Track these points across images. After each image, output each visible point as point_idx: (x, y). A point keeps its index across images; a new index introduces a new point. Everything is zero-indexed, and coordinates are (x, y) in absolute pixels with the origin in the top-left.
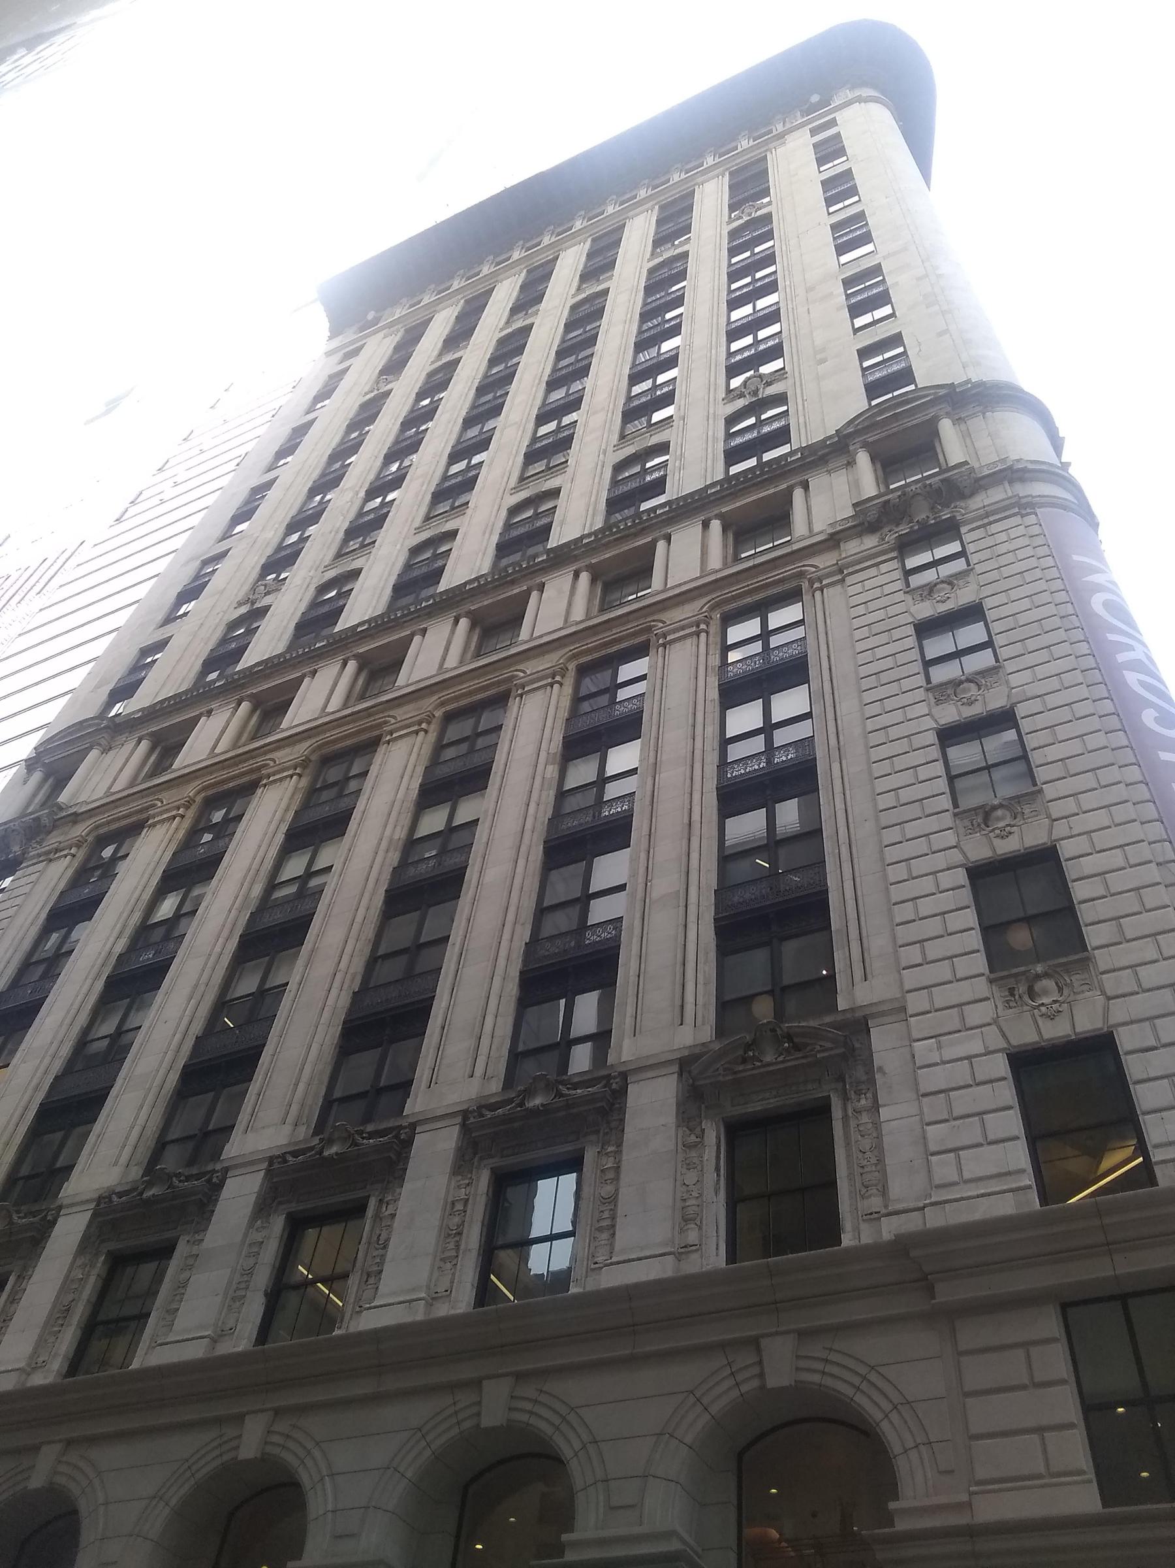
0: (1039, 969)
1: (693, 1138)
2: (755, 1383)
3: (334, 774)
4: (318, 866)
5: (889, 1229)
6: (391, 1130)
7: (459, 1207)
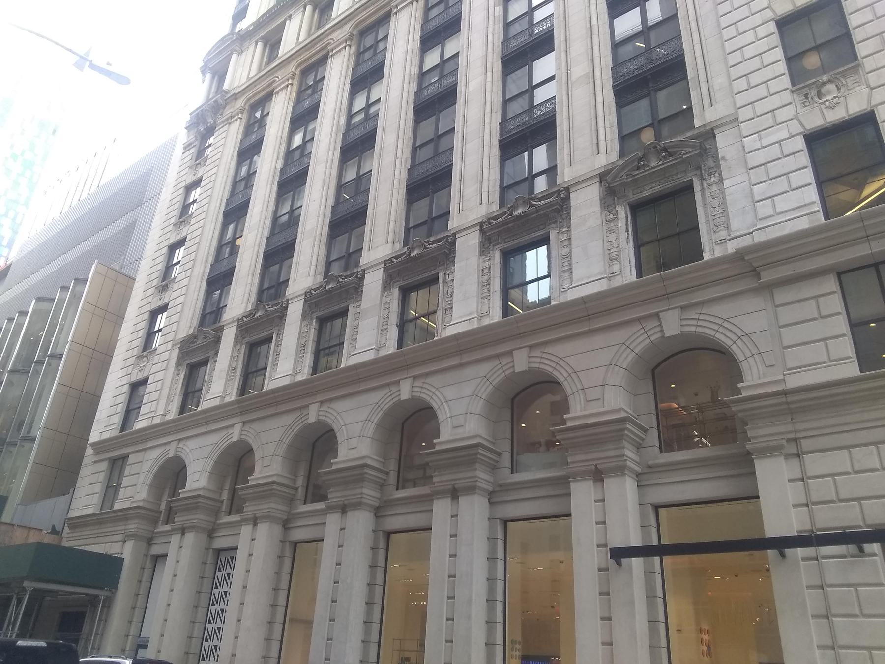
0: (825, 78)
1: (611, 216)
2: (659, 335)
3: (369, 41)
4: (372, 100)
5: (731, 247)
6: (443, 238)
7: (486, 271)
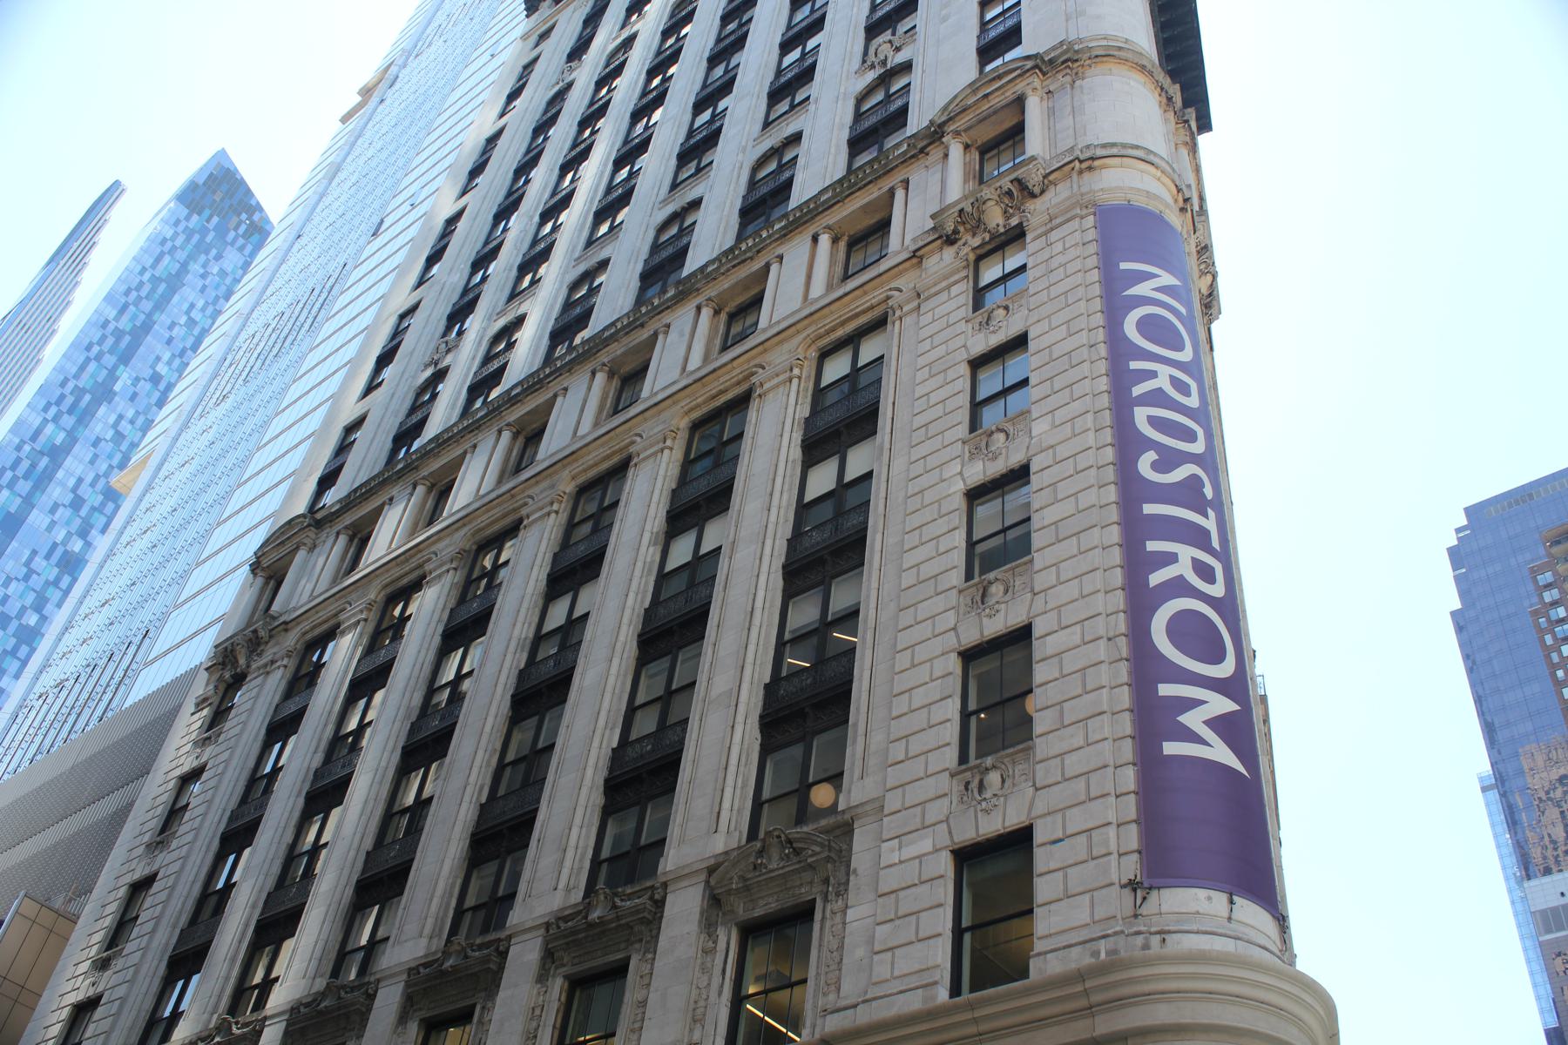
1: (711, 944)
5: (833, 1024)
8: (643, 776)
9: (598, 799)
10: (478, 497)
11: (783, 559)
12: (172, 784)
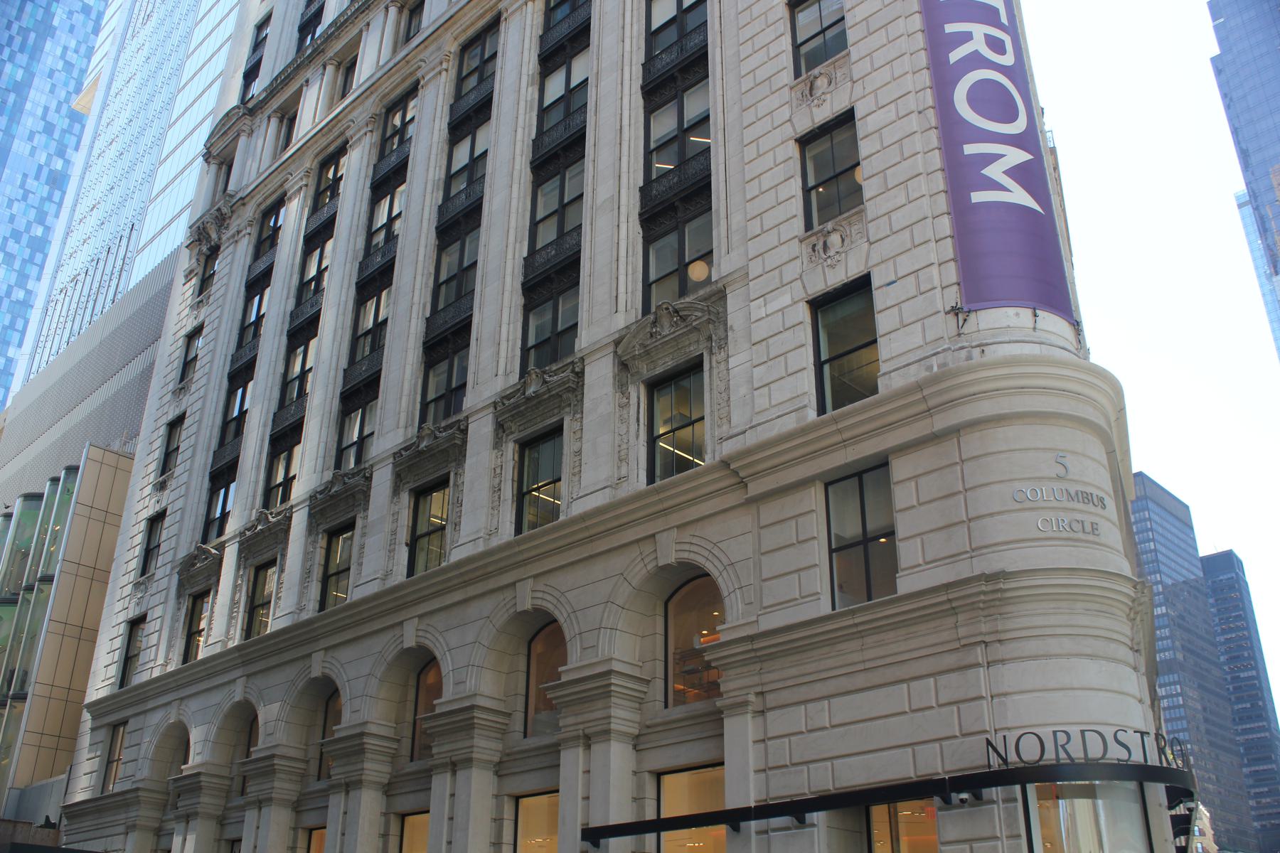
1: (625, 400)
2: (653, 564)
5: (728, 448)
7: (498, 471)
8: (552, 276)
9: (519, 300)
10: (378, 68)
11: (640, 82)
12: (181, 342)
